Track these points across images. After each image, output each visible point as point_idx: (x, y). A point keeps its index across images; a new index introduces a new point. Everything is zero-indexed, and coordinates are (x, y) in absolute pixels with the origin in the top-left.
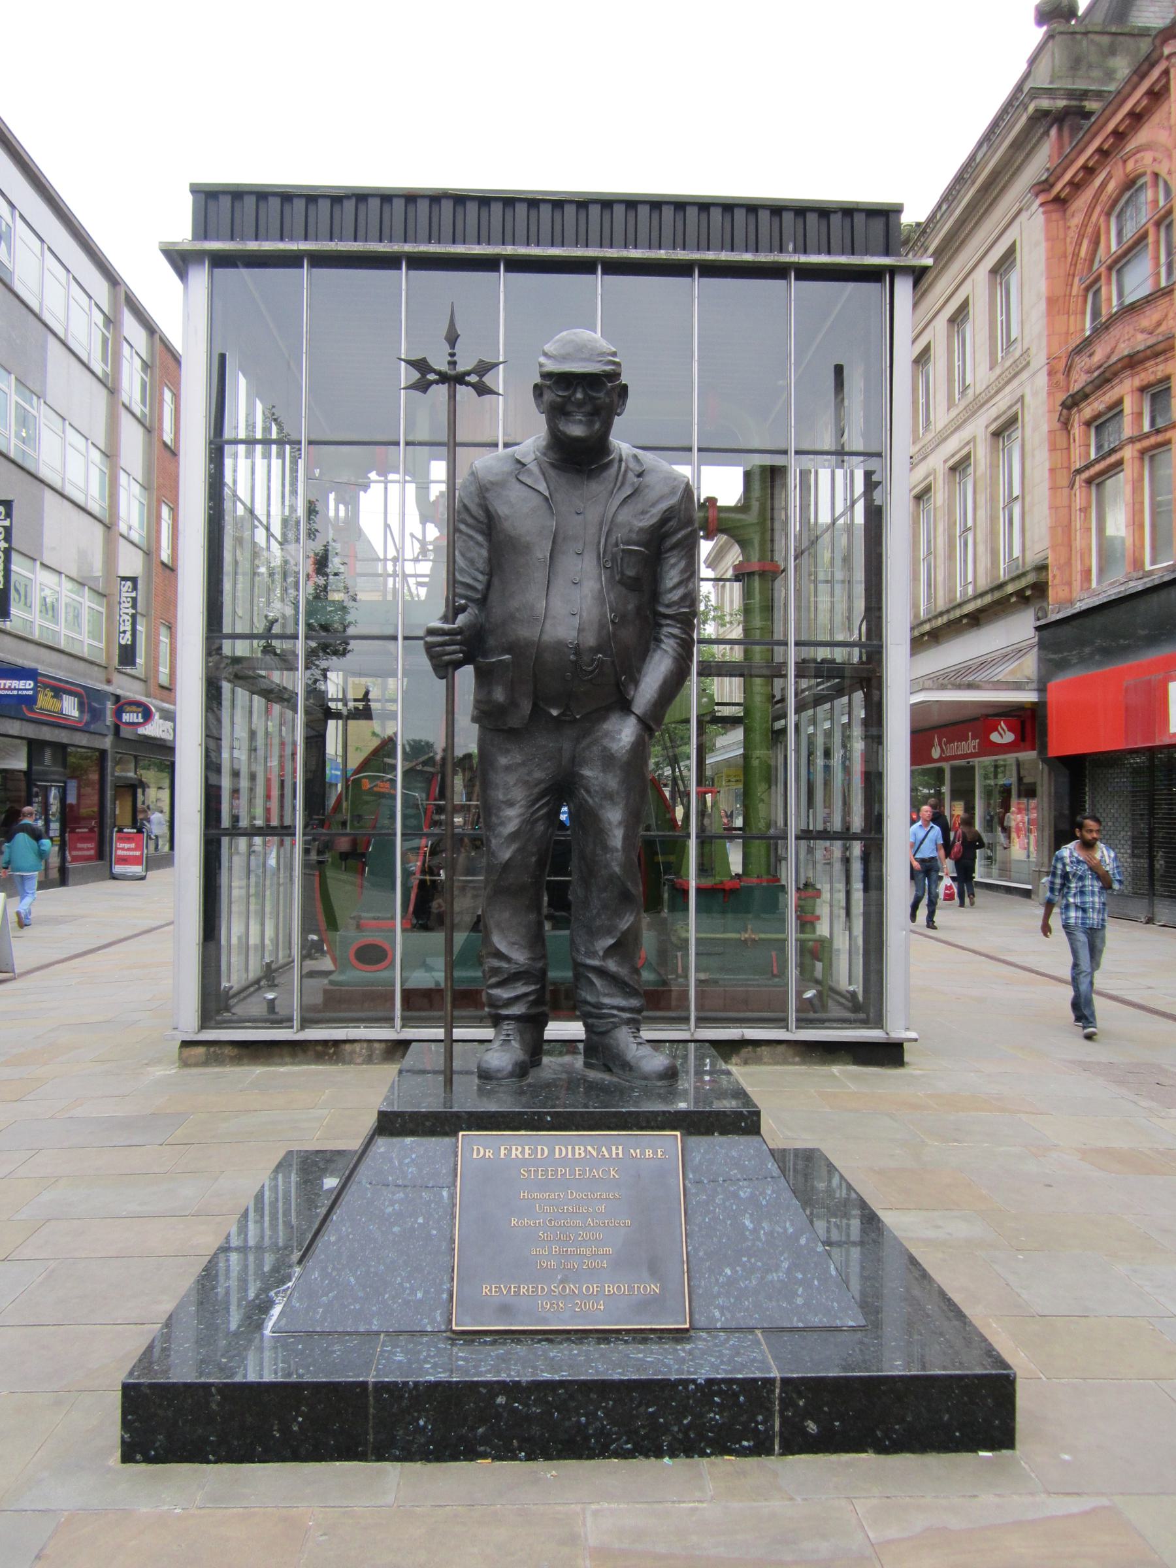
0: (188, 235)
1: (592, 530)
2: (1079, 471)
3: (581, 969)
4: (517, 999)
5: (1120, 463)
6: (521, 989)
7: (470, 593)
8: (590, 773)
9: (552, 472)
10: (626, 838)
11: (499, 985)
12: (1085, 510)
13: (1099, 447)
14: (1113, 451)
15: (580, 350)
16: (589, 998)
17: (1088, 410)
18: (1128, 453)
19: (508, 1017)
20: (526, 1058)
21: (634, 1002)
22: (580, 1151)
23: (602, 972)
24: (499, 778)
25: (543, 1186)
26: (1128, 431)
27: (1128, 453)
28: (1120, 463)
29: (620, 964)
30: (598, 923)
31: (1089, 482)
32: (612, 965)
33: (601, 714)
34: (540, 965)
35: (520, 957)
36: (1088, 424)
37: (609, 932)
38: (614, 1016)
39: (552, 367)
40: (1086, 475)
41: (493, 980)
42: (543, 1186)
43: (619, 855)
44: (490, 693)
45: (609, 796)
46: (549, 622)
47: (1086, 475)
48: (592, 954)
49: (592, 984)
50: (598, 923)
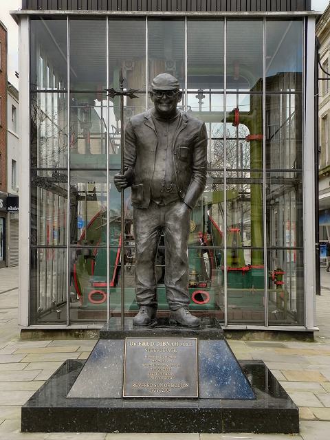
0: (20, 6)
1: (170, 142)
3: (168, 289)
4: (146, 298)
6: (147, 295)
7: (130, 163)
8: (170, 223)
9: (157, 122)
10: (182, 245)
11: (141, 294)
15: (164, 82)
16: (171, 299)
19: (143, 305)
20: (150, 318)
21: (186, 300)
23: (175, 289)
24: (140, 225)
29: (181, 287)
30: (174, 273)
32: (178, 287)
33: (171, 204)
34: (154, 287)
35: (147, 285)
37: (177, 276)
38: (178, 304)
39: (156, 88)
41: (139, 292)
43: (179, 250)
44: (136, 196)
45: (176, 230)
46: (155, 173)
48: (171, 283)
50: (174, 273)
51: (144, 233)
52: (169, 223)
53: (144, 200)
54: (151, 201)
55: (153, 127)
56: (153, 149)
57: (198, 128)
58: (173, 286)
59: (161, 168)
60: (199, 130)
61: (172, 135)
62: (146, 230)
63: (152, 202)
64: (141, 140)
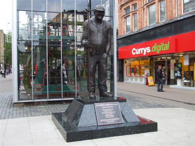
2: (123, 16)
5: (129, 15)
12: (124, 22)
13: (126, 13)
14: (128, 13)
17: (125, 7)
18: (131, 14)
22: (108, 105)
25: (105, 109)
26: (131, 11)
27: (131, 14)
28: (130, 15)
31: (124, 18)
36: (124, 9)
40: (124, 17)
42: (105, 109)
47: (124, 17)
49: (102, 86)
51: (92, 64)
52: (101, 60)
53: (93, 52)
54: (96, 52)
55: (95, 24)
56: (96, 32)
57: (110, 25)
58: (102, 84)
59: (98, 39)
60: (110, 27)
61: (101, 27)
62: (93, 63)
63: (96, 53)
64: (91, 29)
